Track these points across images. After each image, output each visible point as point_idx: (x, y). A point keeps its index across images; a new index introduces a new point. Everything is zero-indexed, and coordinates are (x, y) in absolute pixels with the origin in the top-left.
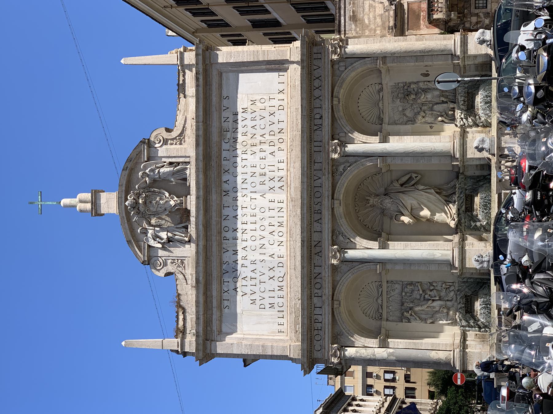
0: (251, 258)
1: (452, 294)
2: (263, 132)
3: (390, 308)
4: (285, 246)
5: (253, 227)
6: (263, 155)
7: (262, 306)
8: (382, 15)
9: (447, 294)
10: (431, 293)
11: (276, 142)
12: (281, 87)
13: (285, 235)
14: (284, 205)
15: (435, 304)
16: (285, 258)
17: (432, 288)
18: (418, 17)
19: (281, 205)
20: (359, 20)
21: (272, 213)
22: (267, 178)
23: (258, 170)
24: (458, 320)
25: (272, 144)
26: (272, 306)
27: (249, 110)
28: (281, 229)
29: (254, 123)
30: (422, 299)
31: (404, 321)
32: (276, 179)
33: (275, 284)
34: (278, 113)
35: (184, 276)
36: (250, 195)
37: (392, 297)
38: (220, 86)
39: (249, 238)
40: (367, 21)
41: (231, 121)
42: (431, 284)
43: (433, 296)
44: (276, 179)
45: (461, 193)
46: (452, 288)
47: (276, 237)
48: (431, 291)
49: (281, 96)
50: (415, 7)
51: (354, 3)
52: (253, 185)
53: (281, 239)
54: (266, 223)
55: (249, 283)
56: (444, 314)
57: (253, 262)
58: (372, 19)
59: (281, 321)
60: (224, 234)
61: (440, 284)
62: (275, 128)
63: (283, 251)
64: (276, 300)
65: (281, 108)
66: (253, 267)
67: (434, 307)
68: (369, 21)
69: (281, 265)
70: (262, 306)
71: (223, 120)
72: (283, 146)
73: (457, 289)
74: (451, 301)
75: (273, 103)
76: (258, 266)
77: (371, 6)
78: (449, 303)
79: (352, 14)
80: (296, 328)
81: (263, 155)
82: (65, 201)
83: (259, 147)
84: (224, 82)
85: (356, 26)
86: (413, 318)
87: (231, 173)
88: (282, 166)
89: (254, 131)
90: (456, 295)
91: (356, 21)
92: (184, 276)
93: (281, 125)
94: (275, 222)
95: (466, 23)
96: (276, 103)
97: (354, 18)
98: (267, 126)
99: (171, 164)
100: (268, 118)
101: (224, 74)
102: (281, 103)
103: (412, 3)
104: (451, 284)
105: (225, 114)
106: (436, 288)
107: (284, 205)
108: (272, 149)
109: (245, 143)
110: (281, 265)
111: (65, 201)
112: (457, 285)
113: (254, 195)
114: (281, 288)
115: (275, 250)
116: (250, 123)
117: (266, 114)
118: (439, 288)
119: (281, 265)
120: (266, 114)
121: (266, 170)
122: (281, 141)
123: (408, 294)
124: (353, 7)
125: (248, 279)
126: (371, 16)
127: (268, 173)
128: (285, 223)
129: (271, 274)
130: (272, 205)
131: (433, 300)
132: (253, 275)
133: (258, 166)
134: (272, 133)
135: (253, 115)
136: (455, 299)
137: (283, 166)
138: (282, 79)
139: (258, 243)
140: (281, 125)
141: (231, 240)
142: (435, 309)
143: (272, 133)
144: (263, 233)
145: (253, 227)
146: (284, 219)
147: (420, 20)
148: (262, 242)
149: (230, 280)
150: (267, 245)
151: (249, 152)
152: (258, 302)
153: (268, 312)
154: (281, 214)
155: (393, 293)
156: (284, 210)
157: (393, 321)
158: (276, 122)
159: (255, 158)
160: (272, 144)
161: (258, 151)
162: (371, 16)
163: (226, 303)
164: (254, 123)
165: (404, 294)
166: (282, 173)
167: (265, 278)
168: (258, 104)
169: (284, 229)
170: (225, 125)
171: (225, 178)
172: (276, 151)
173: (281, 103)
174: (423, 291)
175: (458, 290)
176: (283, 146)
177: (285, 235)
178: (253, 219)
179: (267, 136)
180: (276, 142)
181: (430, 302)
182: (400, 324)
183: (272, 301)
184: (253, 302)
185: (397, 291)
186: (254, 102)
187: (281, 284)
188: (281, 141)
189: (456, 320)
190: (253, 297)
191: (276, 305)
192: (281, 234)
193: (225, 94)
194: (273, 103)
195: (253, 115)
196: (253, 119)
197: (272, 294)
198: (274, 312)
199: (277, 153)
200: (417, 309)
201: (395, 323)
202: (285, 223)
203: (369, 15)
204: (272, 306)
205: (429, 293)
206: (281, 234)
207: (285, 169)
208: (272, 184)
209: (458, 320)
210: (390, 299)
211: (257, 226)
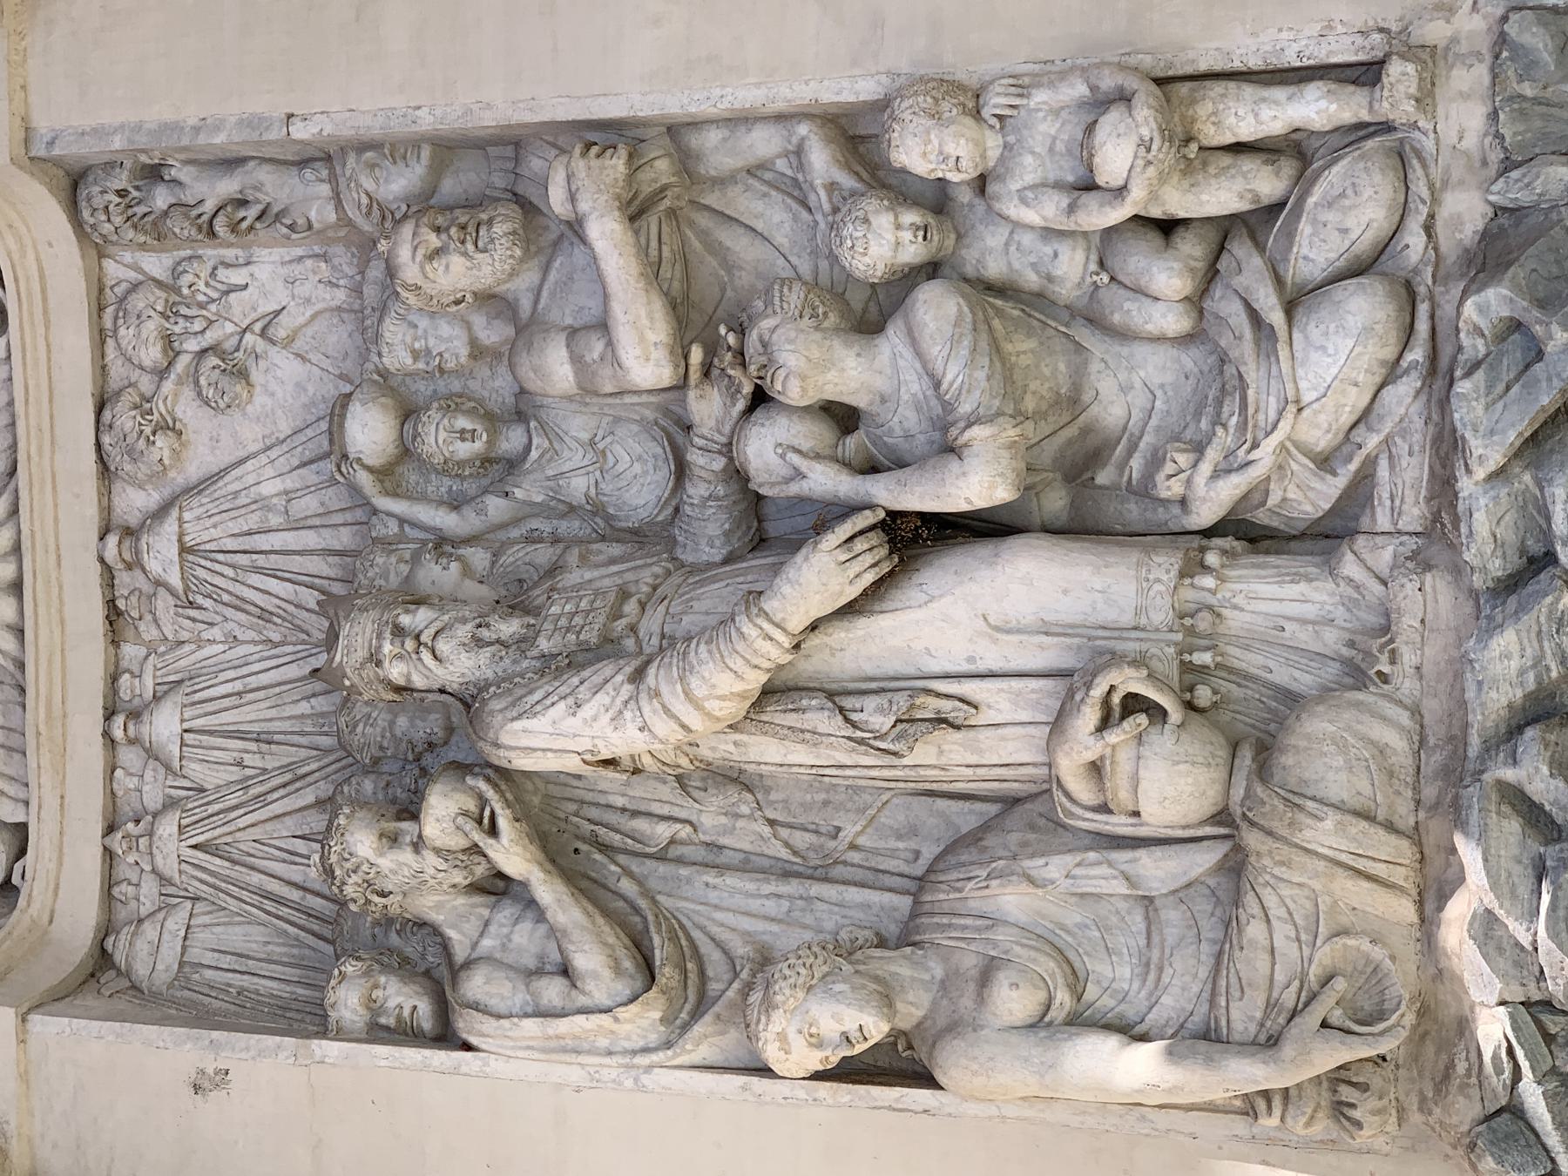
1: (1336, 362)
3: (165, 725)
9: (1221, 390)
10: (851, 372)
15: (960, 617)
17: (882, 242)
24: (1493, 1029)
30: (709, 531)
31: (347, 1001)
37: (202, 523)
42: (857, 136)
43: (904, 422)
46: (1348, 211)
48: (871, 311)
56: (1159, 871)
61: (1047, 119)
67: (924, 705)
73: (1466, 212)
74: (1326, 536)
78: (1272, 606)
86: (525, 939)
90: (1439, 375)
104: (1315, 109)
106: (992, 253)
112: (1462, 120)
118: (1026, 234)
123: (443, 438)
131: (916, 539)
136: (1402, 495)
142: (941, 756)
155: (208, 440)
157: (191, 1004)
165: (370, 431)
174: (712, 329)
175: (1488, 258)
181: (822, 575)
182: (266, 1066)
185: (284, 386)
189: (1443, 1028)
200: (551, 736)
201: (172, 1052)
205: (814, 363)
209: (1493, 1029)
210: (161, 554)
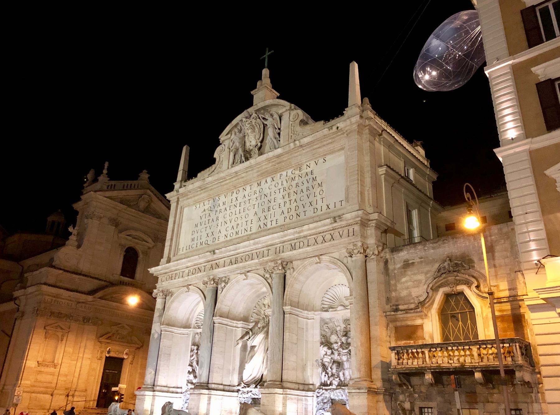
0: (221, 216)
2: (298, 200)
5: (238, 212)
6: (282, 205)
11: (290, 214)
18: (409, 337)
20: (405, 271)
21: (244, 223)
26: (193, 240)
29: (305, 190)
34: (312, 208)
36: (257, 203)
38: (332, 152)
40: (404, 280)
41: (307, 171)
47: (230, 231)
49: (324, 207)
50: (419, 333)
53: (229, 236)
54: (239, 222)
58: (406, 285)
59: (185, 248)
64: (196, 242)
68: (404, 283)
72: (287, 220)
75: (320, 202)
76: (215, 224)
77: (420, 281)
79: (410, 262)
81: (282, 205)
82: (265, 72)
84: (337, 154)
85: (399, 268)
91: (404, 268)
93: (302, 214)
94: (240, 228)
95: (403, 395)
97: (407, 265)
98: (302, 202)
99: (279, 134)
100: (307, 201)
101: (343, 151)
103: (422, 329)
107: (249, 233)
108: (286, 212)
111: (265, 72)
113: (256, 206)
115: (224, 233)
121: (272, 211)
124: (418, 262)
126: (410, 284)
127: (270, 213)
129: (210, 235)
130: (249, 223)
135: (311, 188)
138: (338, 205)
139: (228, 218)
140: (302, 214)
146: (240, 235)
147: (405, 340)
149: (210, 205)
153: (190, 237)
154: (243, 230)
158: (305, 209)
159: (281, 199)
161: (285, 200)
164: (305, 190)
166: (269, 226)
169: (234, 237)
171: (269, 179)
173: (319, 209)
176: (287, 220)
177: (231, 238)
179: (295, 204)
191: (193, 242)
193: (328, 158)
194: (320, 202)
195: (311, 188)
196: (308, 189)
197: (199, 238)
199: (283, 216)
202: (238, 236)
203: (410, 281)
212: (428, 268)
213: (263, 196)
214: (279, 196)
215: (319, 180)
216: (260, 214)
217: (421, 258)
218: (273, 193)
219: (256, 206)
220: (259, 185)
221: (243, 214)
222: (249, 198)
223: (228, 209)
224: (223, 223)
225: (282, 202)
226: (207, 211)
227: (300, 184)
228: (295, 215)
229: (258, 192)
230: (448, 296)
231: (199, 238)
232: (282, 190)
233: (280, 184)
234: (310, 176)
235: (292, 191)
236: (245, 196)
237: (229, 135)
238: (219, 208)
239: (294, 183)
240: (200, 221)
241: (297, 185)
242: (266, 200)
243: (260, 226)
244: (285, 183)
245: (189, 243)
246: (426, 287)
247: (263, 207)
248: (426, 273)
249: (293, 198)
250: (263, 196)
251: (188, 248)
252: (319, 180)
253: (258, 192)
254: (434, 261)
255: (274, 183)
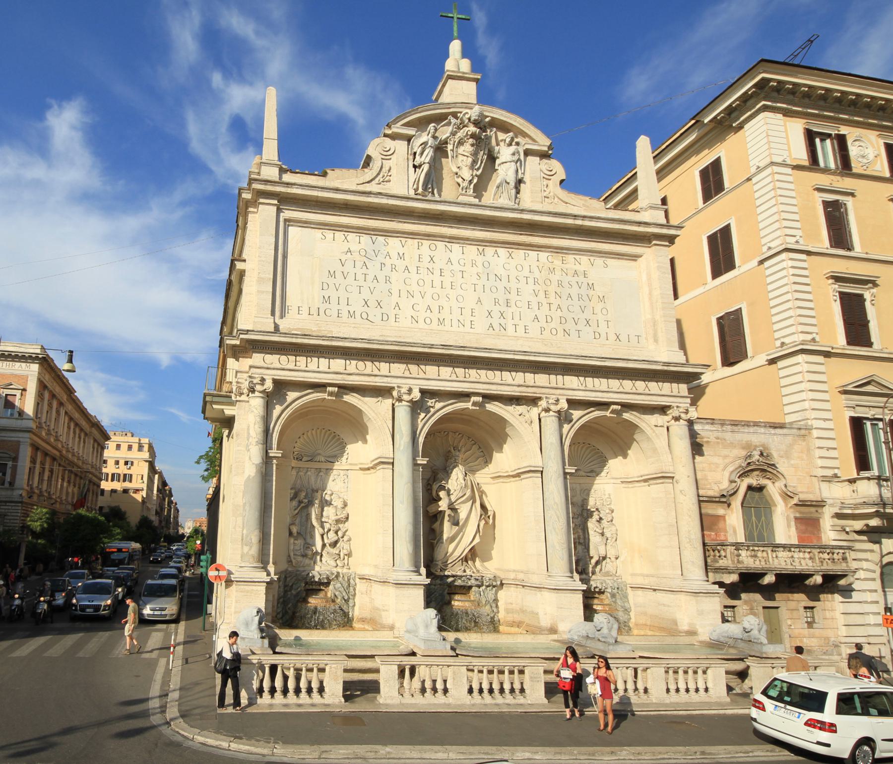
0: (394, 276)
2: (564, 308)
4: (412, 326)
5: (437, 284)
6: (534, 305)
7: (325, 286)
8: (707, 480)
11: (553, 325)
12: (623, 337)
13: (426, 327)
14: (467, 328)
16: (393, 324)
19: (468, 324)
22: (503, 308)
23: (513, 297)
25: (549, 319)
26: (327, 300)
27: (591, 292)
28: (435, 321)
29: (575, 297)
32: (502, 321)
33: (357, 306)
35: (368, 182)
39: (421, 276)
44: (502, 321)
45: (477, 580)
49: (612, 337)
51: (718, 443)
52: (494, 290)
53: (421, 321)
54: (443, 302)
55: (360, 272)
57: (388, 280)
59: (305, 311)
60: (426, 243)
62: (570, 325)
63: (405, 322)
64: (334, 307)
65: (597, 335)
66: (381, 279)
69: (385, 317)
70: (325, 286)
71: (577, 257)
75: (603, 325)
80: (296, 330)
81: (534, 305)
83: (544, 301)
87: (508, 261)
88: (520, 329)
89: (564, 297)
92: (368, 182)
93: (574, 333)
94: (445, 314)
96: (603, 328)
99: (519, 182)
102: (603, 336)
105: (584, 259)
108: (542, 319)
109: (548, 282)
110: (385, 318)
113: (479, 288)
114: (351, 315)
116: (574, 291)
117: (588, 314)
119: (385, 317)
120: (588, 314)
121: (513, 308)
122: (554, 332)
125: (364, 270)
126: (704, 465)
127: (510, 310)
128: (440, 327)
132: (370, 278)
133: (519, 298)
134: (563, 321)
135: (585, 298)
137: (520, 329)
139: (414, 288)
140: (574, 333)
141: (419, 252)
143: (563, 321)
144: (428, 296)
145: (437, 284)
148: (417, 296)
150: (413, 301)
151: (537, 287)
152: (331, 281)
154: (455, 322)
156: (461, 329)
158: (579, 327)
160: (549, 319)
162: (704, 465)
163: (329, 234)
164: (575, 297)
166: (510, 330)
167: (366, 294)
168: (601, 305)
170: (570, 258)
171: (502, 251)
172: (540, 324)
173: (603, 336)
176: (546, 333)
178: (447, 285)
179: (559, 313)
180: (553, 325)
183: (334, 300)
184: (332, 274)
186: (602, 299)
187: (358, 315)
188: (554, 332)
190: (339, 275)
191: (327, 305)
192: (428, 321)
193: (610, 262)
194: (603, 325)
195: (585, 298)
196: (580, 298)
197: (343, 301)
198: (317, 303)
204: (327, 300)
206: (428, 321)
207: (516, 334)
208: (496, 314)
211: (438, 290)
212: (725, 452)
213: (492, 277)
214: (527, 290)
215: (599, 290)
216: (488, 305)
217: (717, 438)
218: (512, 278)
219: (479, 288)
220: (482, 253)
221: (453, 294)
222: (462, 269)
223: (413, 269)
224: (404, 294)
225: (534, 301)
226: (356, 255)
227: (565, 284)
228: (560, 332)
229: (480, 264)
230: (750, 488)
231: (343, 301)
232: (531, 281)
233: (527, 269)
234: (581, 279)
235: (552, 289)
236: (449, 260)
237: (411, 131)
238: (388, 262)
239: (555, 278)
240: (339, 268)
241: (560, 284)
242: (501, 285)
243: (491, 326)
244: (536, 271)
245: (317, 303)
246: (726, 474)
247: (495, 296)
248: (725, 457)
249: (555, 302)
250: (492, 277)
251: (314, 311)
252: (599, 290)
253: (480, 264)
254: (732, 445)
255: (513, 263)
